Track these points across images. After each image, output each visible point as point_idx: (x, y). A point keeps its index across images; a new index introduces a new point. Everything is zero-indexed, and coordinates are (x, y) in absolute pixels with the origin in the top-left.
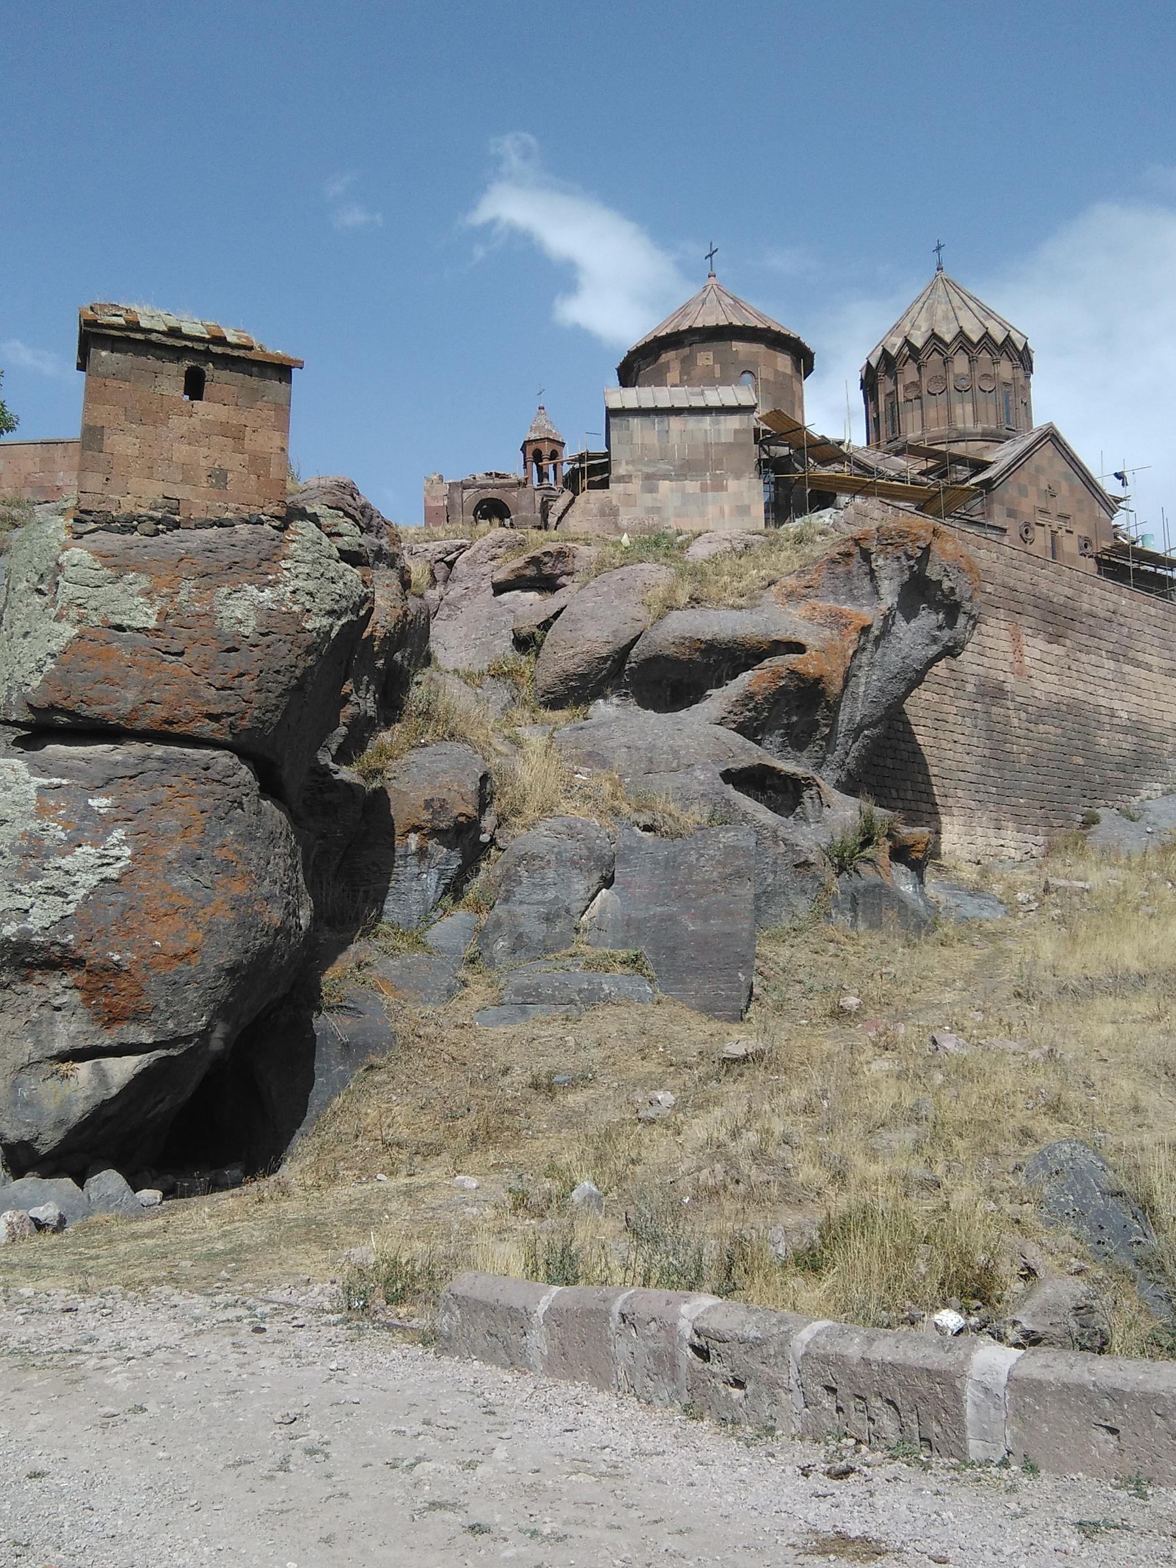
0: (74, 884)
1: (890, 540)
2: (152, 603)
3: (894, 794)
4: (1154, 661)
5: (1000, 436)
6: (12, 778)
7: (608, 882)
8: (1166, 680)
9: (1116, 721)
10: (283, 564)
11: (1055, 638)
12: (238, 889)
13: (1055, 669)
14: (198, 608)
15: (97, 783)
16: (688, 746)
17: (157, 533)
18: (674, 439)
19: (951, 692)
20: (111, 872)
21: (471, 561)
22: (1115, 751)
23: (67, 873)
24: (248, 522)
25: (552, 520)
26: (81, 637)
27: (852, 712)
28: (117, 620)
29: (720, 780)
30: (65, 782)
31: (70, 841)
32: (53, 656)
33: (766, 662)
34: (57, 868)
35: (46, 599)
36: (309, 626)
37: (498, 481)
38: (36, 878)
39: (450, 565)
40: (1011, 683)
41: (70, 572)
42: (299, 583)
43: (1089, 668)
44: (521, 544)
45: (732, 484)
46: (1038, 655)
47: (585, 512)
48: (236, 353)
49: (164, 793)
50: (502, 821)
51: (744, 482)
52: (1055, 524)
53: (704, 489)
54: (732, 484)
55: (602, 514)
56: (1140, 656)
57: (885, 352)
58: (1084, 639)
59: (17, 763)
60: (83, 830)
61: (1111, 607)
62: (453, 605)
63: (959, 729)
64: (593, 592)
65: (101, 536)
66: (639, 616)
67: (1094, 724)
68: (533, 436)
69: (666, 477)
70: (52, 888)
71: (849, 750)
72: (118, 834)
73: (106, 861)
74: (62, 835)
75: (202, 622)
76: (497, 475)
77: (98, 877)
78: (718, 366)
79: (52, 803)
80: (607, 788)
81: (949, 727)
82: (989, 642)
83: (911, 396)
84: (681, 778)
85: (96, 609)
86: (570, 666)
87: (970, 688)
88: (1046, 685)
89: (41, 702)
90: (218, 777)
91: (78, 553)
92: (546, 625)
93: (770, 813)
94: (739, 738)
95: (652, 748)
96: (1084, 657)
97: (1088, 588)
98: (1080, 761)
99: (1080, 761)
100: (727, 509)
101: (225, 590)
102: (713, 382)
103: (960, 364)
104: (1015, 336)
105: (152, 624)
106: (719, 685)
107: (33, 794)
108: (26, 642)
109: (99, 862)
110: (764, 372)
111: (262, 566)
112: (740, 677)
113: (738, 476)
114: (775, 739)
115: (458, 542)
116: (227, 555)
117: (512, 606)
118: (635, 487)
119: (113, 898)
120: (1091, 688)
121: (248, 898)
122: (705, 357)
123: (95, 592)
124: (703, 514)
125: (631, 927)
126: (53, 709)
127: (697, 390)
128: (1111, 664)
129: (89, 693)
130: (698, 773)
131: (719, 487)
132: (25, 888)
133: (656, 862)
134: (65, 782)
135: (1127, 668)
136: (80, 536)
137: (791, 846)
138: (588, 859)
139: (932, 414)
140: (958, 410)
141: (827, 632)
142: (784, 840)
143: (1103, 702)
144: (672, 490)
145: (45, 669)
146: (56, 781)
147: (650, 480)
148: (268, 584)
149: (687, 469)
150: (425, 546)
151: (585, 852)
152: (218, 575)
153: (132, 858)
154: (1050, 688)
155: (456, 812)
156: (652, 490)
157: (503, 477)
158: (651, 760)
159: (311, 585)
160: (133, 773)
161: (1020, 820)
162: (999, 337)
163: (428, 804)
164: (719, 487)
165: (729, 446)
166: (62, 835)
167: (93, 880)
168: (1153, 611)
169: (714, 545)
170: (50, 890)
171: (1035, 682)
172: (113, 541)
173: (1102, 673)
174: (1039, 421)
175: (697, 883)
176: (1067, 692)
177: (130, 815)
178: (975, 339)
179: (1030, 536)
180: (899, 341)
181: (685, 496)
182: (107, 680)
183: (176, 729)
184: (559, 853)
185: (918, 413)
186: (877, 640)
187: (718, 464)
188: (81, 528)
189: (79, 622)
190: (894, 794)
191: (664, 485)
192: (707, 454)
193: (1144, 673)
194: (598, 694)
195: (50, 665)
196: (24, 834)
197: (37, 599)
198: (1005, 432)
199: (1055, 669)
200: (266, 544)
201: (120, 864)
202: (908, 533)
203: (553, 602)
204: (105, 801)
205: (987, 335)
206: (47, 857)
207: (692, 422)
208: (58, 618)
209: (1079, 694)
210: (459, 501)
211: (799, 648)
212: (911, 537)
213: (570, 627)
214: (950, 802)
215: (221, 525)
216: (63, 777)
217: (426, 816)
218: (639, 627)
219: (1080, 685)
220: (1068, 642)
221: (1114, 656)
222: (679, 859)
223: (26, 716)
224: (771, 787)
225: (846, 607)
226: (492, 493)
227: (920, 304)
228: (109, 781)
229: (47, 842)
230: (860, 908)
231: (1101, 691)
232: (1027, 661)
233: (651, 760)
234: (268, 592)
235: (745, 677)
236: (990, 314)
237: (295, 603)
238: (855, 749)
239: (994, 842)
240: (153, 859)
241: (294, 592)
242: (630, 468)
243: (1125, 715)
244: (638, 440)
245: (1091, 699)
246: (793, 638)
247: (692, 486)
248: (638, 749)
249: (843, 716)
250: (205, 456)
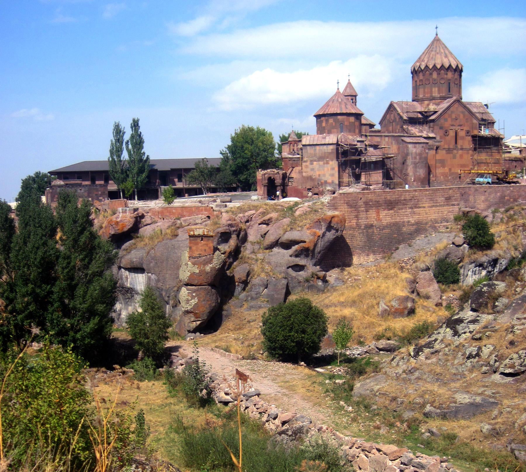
7: (266, 288)
11: (391, 209)
18: (317, 151)
21: (255, 217)
25: (288, 175)
27: (318, 249)
45: (331, 163)
46: (384, 214)
47: (295, 173)
50: (251, 278)
53: (324, 164)
54: (331, 163)
55: (299, 173)
56: (421, 205)
58: (401, 207)
61: (412, 196)
69: (315, 161)
71: (318, 256)
80: (270, 269)
82: (369, 216)
83: (421, 84)
84: (281, 269)
86: (268, 243)
87: (362, 227)
96: (400, 211)
97: (404, 194)
98: (396, 236)
110: (346, 123)
113: (332, 160)
114: (302, 256)
118: (308, 163)
124: (324, 170)
125: (268, 296)
128: (410, 210)
135: (415, 210)
137: (298, 279)
143: (405, 220)
147: (312, 162)
154: (387, 221)
156: (312, 164)
161: (374, 253)
165: (330, 153)
173: (406, 213)
181: (320, 165)
186: (322, 238)
191: (315, 163)
193: (422, 209)
194: (273, 248)
203: (269, 228)
207: (321, 147)
209: (397, 220)
219: (398, 218)
221: (412, 208)
227: (425, 54)
231: (405, 218)
232: (381, 217)
238: (319, 255)
244: (309, 152)
245: (402, 220)
247: (321, 163)
249: (316, 251)
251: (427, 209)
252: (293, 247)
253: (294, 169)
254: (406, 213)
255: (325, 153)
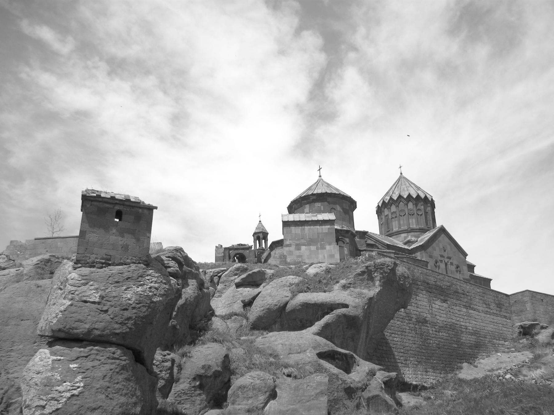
0: (62, 396)
1: (378, 267)
2: (98, 293)
3: (387, 360)
4: (481, 308)
5: (424, 230)
6: (44, 356)
8: (485, 315)
9: (468, 330)
10: (147, 278)
11: (445, 301)
12: (123, 399)
13: (444, 312)
14: (114, 294)
15: (73, 359)
16: (305, 344)
17: (101, 268)
19: (407, 322)
20: (75, 392)
22: (469, 342)
23: (60, 392)
24: (135, 263)
26: (71, 305)
28: (85, 299)
29: (316, 356)
30: (62, 358)
31: (62, 380)
32: (61, 312)
33: (334, 312)
34: (56, 391)
35: (62, 291)
36: (155, 300)
37: (242, 247)
38: (49, 394)
39: (220, 277)
40: (429, 317)
41: (70, 282)
42: (152, 285)
43: (457, 311)
44: (245, 270)
45: (328, 247)
46: (437, 307)
47: (274, 258)
48: (134, 205)
49: (96, 363)
51: (332, 246)
52: (446, 260)
53: (317, 249)
54: (328, 247)
57: (384, 202)
59: (47, 351)
60: (67, 376)
62: (221, 292)
63: (409, 335)
64: (271, 286)
65: (83, 269)
66: (288, 295)
67: (460, 332)
68: (257, 231)
69: (304, 245)
70: (54, 398)
72: (79, 378)
73: (74, 388)
74: (59, 378)
75: (115, 299)
76: (242, 245)
77: (71, 394)
78: (322, 207)
79: (57, 366)
81: (406, 334)
83: (394, 216)
85: (78, 295)
87: (414, 320)
88: (442, 318)
89: (55, 328)
90: (117, 357)
91: (74, 275)
92: (254, 298)
93: (336, 368)
94: (324, 340)
95: (291, 345)
96: (455, 308)
98: (456, 346)
99: (456, 346)
100: (326, 256)
101: (124, 288)
102: (320, 212)
103: (411, 205)
104: (428, 196)
105: (97, 300)
106: (319, 319)
107: (50, 362)
108: (54, 307)
109: (71, 388)
111: (138, 279)
112: (325, 317)
113: (330, 244)
115: (223, 269)
116: (126, 275)
117: (241, 292)
118: (292, 248)
119: (75, 402)
120: (458, 319)
121: (127, 403)
122: (318, 205)
123: (78, 289)
124: (317, 258)
126: (60, 330)
127: (314, 214)
128: (465, 310)
129: (73, 325)
130: (308, 354)
131: (323, 248)
132: (44, 398)
133: (291, 389)
134: (62, 358)
136: (75, 269)
138: (265, 387)
139: (402, 222)
140: (410, 221)
141: (357, 300)
142: (341, 379)
144: (306, 249)
145: (58, 316)
146: (59, 358)
148: (141, 285)
149: (311, 242)
150: (211, 270)
151: (264, 385)
152: (123, 282)
153: (84, 387)
154: (442, 319)
155: (213, 370)
156: (299, 249)
157: (245, 245)
158: (290, 349)
159: (156, 285)
160: (86, 355)
162: (423, 196)
163: (203, 367)
164: (323, 248)
165: (326, 234)
166: (59, 378)
167: (68, 395)
168: (478, 290)
169: (316, 269)
170: (53, 399)
171: (438, 317)
172: (86, 271)
173: (462, 313)
174: (438, 224)
175: (306, 396)
176: (450, 320)
177: (84, 371)
178: (414, 196)
179: (438, 264)
180: (388, 198)
182: (79, 321)
183: (103, 339)
184: (254, 385)
185: (397, 222)
187: (322, 240)
188: (76, 266)
189: (72, 299)
190: (387, 360)
191: (303, 248)
192: (318, 236)
193: (477, 313)
195: (60, 315)
196: (46, 377)
197: (59, 291)
198: (426, 228)
199: (444, 312)
200: (141, 271)
201: (79, 390)
202: (385, 264)
203: (256, 291)
204: (75, 365)
205: (418, 196)
206: (53, 386)
208: (64, 298)
210: (228, 254)
211: (346, 306)
212: (386, 265)
213: (262, 299)
214: (408, 362)
215: (126, 264)
216: (62, 356)
217: (203, 371)
218: (287, 299)
220: (448, 302)
221: (465, 306)
222: (300, 387)
223: (50, 334)
224: (337, 358)
225: (365, 291)
226: (241, 251)
228: (78, 358)
229: (53, 381)
230: (370, 404)
232: (434, 309)
233: (290, 349)
234: (140, 289)
235: (327, 318)
236: (419, 188)
237: (150, 292)
239: (425, 377)
240: (91, 388)
241: (150, 288)
242: (291, 242)
243: (471, 328)
244: (293, 232)
246: (344, 302)
247: (313, 248)
248: (286, 345)
250: (120, 241)
251: (483, 315)
252: (317, 323)
253: (272, 253)
254: (462, 313)
255: (318, 233)
